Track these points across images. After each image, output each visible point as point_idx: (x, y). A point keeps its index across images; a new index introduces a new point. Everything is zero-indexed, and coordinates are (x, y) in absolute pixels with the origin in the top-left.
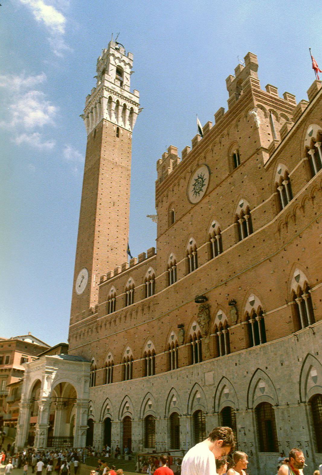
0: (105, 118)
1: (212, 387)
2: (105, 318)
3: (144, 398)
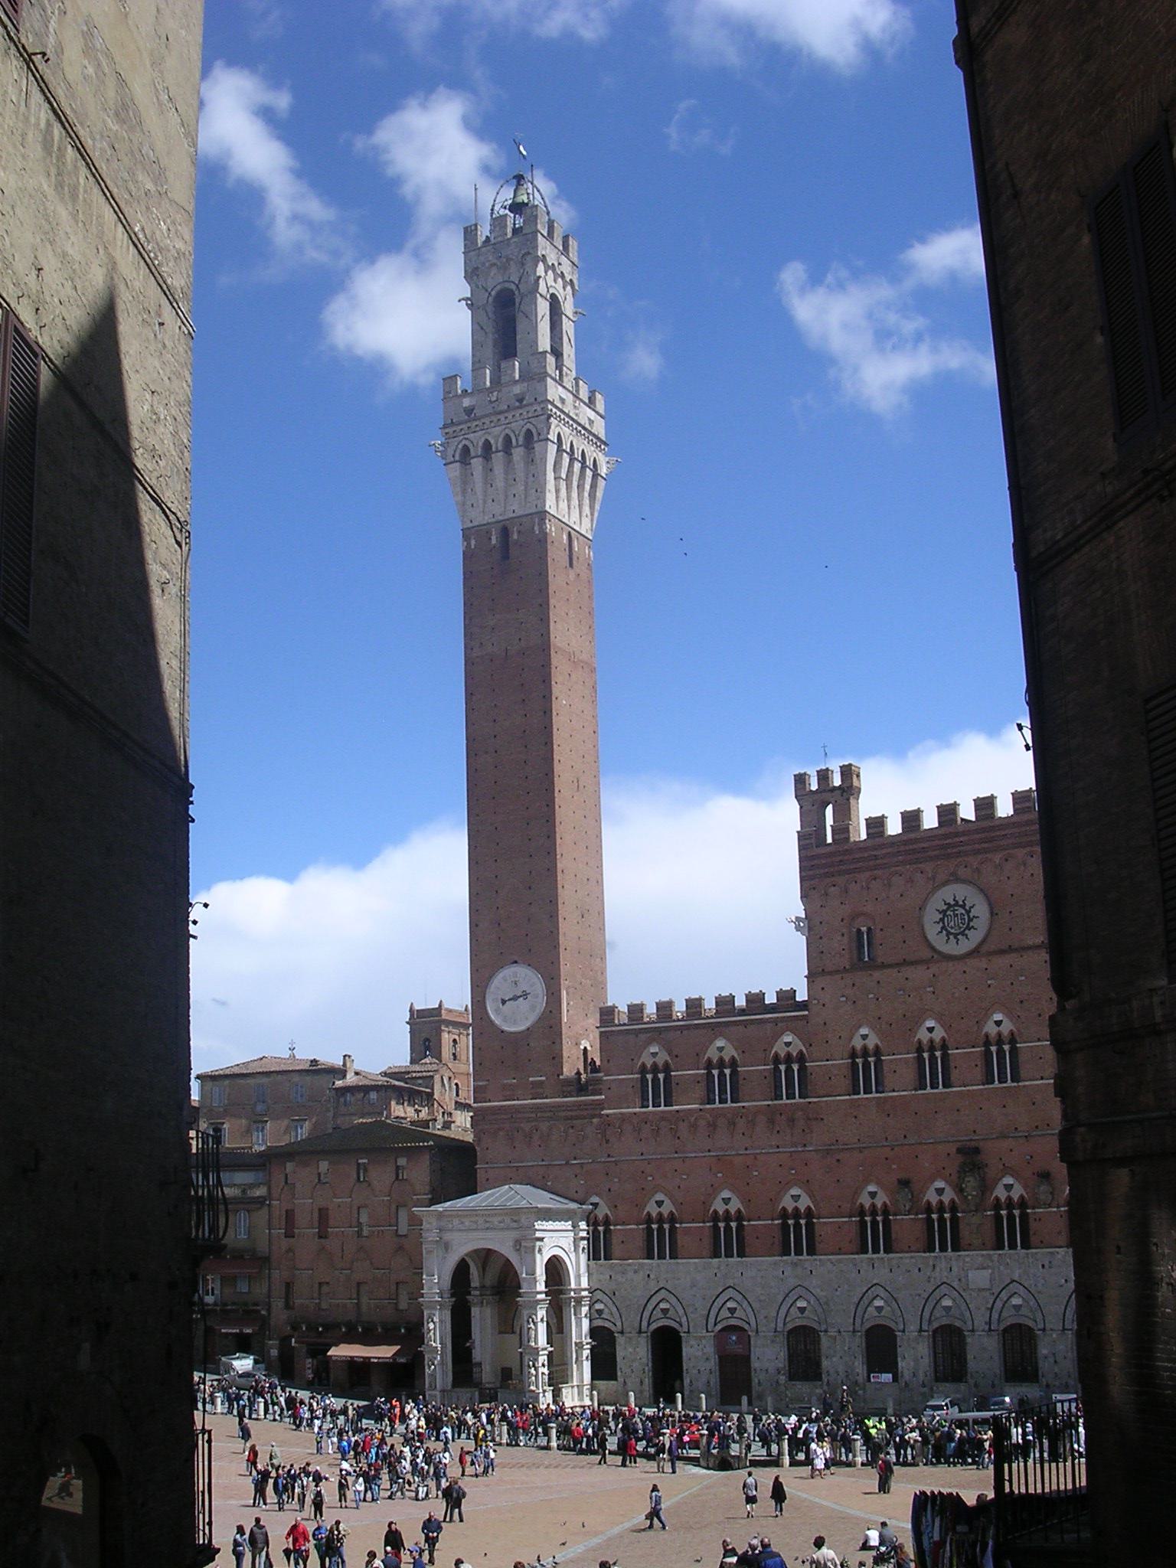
0: (547, 508)
1: (987, 1294)
3: (787, 1295)
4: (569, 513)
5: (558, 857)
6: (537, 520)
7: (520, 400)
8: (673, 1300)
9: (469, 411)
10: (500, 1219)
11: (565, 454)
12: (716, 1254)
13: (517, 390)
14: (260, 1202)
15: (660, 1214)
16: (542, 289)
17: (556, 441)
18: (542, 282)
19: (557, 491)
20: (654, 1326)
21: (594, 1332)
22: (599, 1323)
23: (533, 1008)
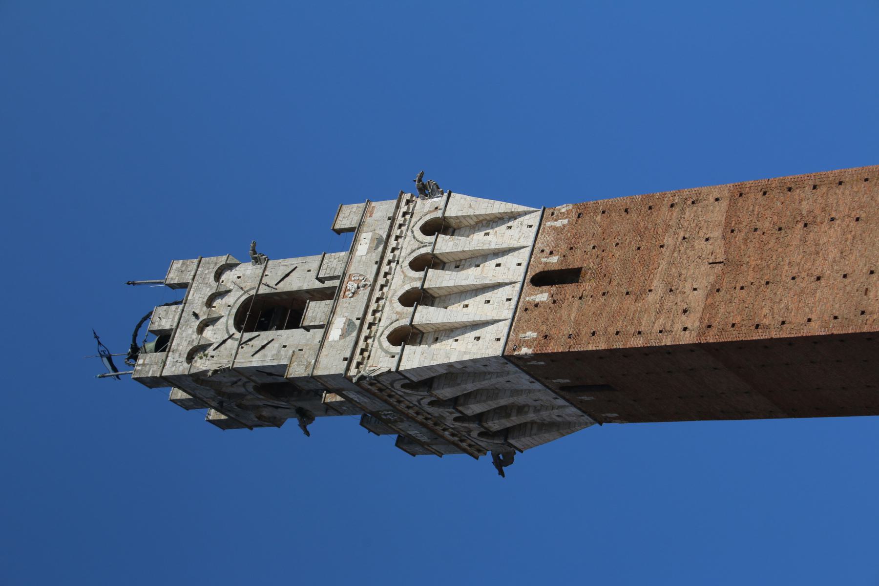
6: (549, 224)
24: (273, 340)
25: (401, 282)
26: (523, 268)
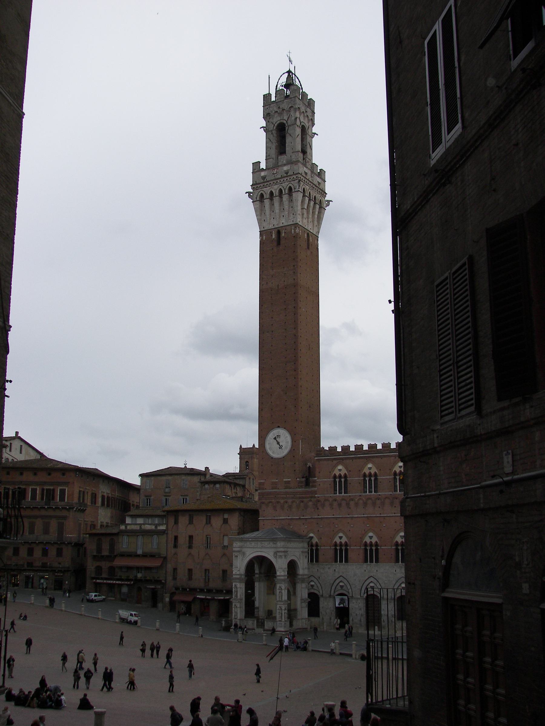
2: (331, 497)
3: (397, 581)
4: (308, 224)
5: (299, 380)
6: (293, 227)
7: (287, 173)
8: (346, 582)
9: (264, 178)
10: (268, 543)
11: (307, 197)
12: (366, 561)
13: (285, 168)
14: (163, 532)
15: (341, 542)
16: (298, 123)
17: (302, 192)
18: (298, 120)
19: (303, 214)
20: (337, 593)
21: (311, 595)
22: (312, 591)
23: (286, 448)
24: (272, 143)
25: (275, 188)
26: (282, 225)
